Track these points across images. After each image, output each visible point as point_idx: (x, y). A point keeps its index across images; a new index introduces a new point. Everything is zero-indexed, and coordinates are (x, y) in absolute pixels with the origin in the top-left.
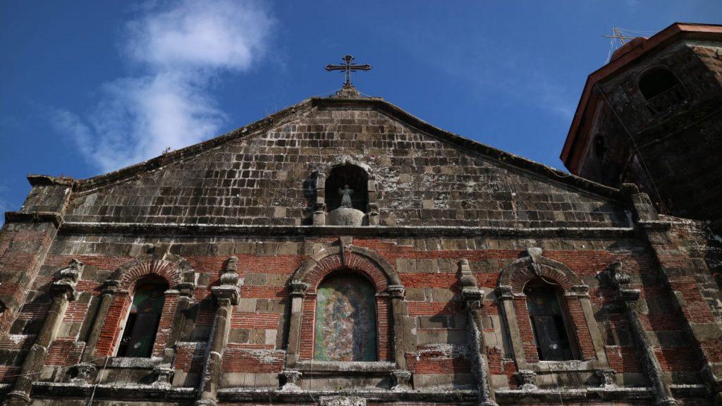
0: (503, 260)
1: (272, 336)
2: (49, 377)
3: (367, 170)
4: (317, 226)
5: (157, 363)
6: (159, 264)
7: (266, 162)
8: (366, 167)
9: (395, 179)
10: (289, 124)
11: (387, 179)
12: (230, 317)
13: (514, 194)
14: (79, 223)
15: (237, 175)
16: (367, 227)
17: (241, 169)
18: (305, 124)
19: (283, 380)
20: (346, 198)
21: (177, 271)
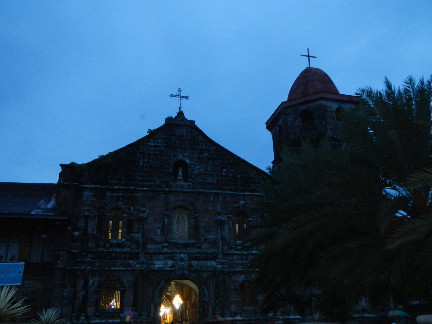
0: (231, 204)
1: (159, 231)
2: (91, 247)
3: (188, 164)
4: (172, 190)
5: (124, 242)
6: (118, 204)
7: (151, 157)
8: (188, 161)
9: (198, 167)
10: (158, 136)
11: (195, 167)
12: (145, 225)
13: (239, 176)
14: (85, 186)
15: (141, 163)
16: (188, 191)
17: (142, 159)
18: (164, 136)
19: (163, 247)
20: (180, 173)
21: (125, 207)
